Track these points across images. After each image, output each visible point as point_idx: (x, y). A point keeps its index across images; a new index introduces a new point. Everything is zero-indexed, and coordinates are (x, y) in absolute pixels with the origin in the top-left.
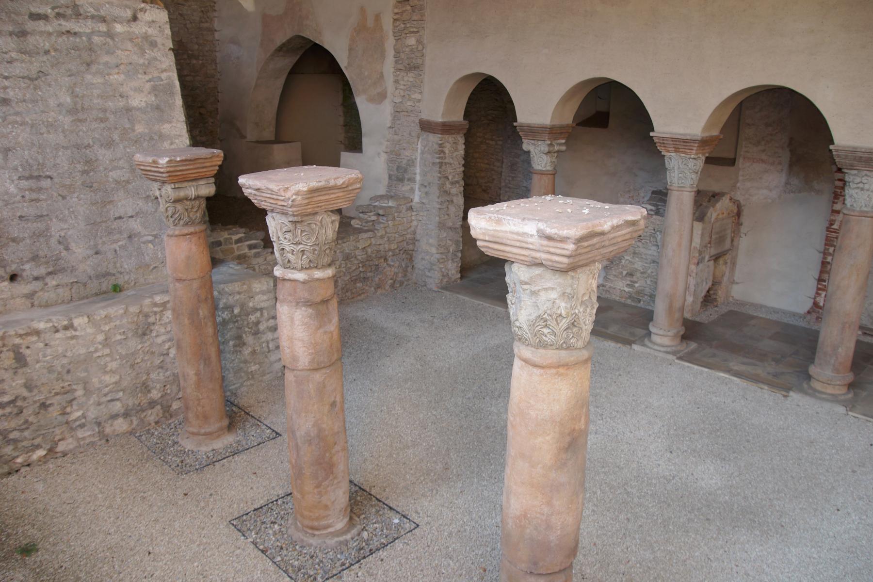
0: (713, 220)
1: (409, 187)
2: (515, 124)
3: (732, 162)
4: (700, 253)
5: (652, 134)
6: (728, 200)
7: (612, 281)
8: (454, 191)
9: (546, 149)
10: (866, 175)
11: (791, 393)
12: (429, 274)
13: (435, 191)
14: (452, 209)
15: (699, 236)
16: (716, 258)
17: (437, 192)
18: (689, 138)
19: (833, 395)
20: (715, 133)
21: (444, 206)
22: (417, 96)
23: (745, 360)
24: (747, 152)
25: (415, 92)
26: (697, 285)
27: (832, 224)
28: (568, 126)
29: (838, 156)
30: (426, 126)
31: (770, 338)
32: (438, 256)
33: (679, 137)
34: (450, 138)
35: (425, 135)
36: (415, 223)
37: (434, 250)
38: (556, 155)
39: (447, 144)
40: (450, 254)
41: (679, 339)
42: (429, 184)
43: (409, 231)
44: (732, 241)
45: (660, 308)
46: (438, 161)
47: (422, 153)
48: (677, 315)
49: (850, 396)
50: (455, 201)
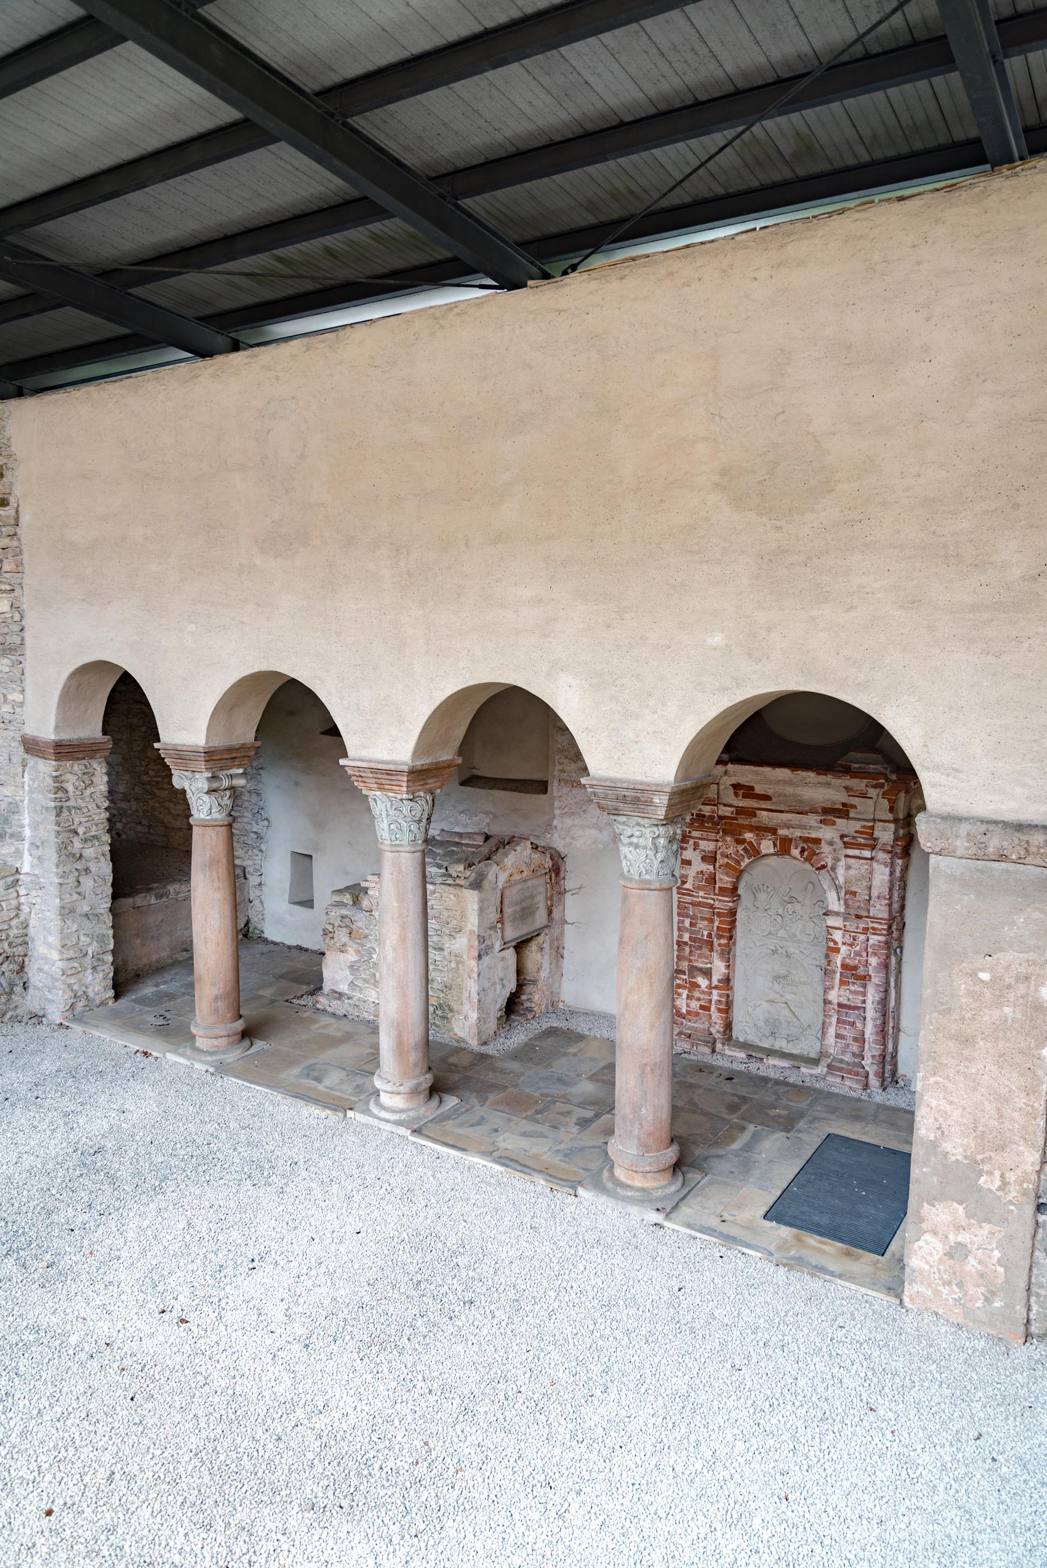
0: (500, 885)
1: (13, 849)
2: (156, 745)
3: (542, 787)
4: (481, 939)
5: (342, 762)
6: (529, 850)
7: (361, 989)
8: (89, 852)
9: (205, 786)
10: (638, 824)
11: (581, 1191)
12: (50, 997)
13: (51, 854)
14: (88, 883)
15: (476, 913)
16: (520, 946)
17: (54, 857)
18: (392, 767)
19: (643, 1190)
20: (447, 755)
21: (71, 879)
22: (17, 697)
24: (563, 771)
25: (14, 690)
26: (482, 991)
27: (684, 883)
28: (243, 747)
30: (32, 747)
31: (590, 1078)
32: (60, 964)
33: (380, 766)
34: (77, 767)
35: (32, 761)
36: (25, 909)
37: (55, 955)
38: (228, 793)
39: (69, 776)
40: (88, 959)
41: (422, 1097)
42: (43, 843)
43: (14, 923)
45: (386, 1042)
46: (53, 804)
47: (31, 792)
48: (414, 1056)
49: (673, 1188)
50: (93, 869)
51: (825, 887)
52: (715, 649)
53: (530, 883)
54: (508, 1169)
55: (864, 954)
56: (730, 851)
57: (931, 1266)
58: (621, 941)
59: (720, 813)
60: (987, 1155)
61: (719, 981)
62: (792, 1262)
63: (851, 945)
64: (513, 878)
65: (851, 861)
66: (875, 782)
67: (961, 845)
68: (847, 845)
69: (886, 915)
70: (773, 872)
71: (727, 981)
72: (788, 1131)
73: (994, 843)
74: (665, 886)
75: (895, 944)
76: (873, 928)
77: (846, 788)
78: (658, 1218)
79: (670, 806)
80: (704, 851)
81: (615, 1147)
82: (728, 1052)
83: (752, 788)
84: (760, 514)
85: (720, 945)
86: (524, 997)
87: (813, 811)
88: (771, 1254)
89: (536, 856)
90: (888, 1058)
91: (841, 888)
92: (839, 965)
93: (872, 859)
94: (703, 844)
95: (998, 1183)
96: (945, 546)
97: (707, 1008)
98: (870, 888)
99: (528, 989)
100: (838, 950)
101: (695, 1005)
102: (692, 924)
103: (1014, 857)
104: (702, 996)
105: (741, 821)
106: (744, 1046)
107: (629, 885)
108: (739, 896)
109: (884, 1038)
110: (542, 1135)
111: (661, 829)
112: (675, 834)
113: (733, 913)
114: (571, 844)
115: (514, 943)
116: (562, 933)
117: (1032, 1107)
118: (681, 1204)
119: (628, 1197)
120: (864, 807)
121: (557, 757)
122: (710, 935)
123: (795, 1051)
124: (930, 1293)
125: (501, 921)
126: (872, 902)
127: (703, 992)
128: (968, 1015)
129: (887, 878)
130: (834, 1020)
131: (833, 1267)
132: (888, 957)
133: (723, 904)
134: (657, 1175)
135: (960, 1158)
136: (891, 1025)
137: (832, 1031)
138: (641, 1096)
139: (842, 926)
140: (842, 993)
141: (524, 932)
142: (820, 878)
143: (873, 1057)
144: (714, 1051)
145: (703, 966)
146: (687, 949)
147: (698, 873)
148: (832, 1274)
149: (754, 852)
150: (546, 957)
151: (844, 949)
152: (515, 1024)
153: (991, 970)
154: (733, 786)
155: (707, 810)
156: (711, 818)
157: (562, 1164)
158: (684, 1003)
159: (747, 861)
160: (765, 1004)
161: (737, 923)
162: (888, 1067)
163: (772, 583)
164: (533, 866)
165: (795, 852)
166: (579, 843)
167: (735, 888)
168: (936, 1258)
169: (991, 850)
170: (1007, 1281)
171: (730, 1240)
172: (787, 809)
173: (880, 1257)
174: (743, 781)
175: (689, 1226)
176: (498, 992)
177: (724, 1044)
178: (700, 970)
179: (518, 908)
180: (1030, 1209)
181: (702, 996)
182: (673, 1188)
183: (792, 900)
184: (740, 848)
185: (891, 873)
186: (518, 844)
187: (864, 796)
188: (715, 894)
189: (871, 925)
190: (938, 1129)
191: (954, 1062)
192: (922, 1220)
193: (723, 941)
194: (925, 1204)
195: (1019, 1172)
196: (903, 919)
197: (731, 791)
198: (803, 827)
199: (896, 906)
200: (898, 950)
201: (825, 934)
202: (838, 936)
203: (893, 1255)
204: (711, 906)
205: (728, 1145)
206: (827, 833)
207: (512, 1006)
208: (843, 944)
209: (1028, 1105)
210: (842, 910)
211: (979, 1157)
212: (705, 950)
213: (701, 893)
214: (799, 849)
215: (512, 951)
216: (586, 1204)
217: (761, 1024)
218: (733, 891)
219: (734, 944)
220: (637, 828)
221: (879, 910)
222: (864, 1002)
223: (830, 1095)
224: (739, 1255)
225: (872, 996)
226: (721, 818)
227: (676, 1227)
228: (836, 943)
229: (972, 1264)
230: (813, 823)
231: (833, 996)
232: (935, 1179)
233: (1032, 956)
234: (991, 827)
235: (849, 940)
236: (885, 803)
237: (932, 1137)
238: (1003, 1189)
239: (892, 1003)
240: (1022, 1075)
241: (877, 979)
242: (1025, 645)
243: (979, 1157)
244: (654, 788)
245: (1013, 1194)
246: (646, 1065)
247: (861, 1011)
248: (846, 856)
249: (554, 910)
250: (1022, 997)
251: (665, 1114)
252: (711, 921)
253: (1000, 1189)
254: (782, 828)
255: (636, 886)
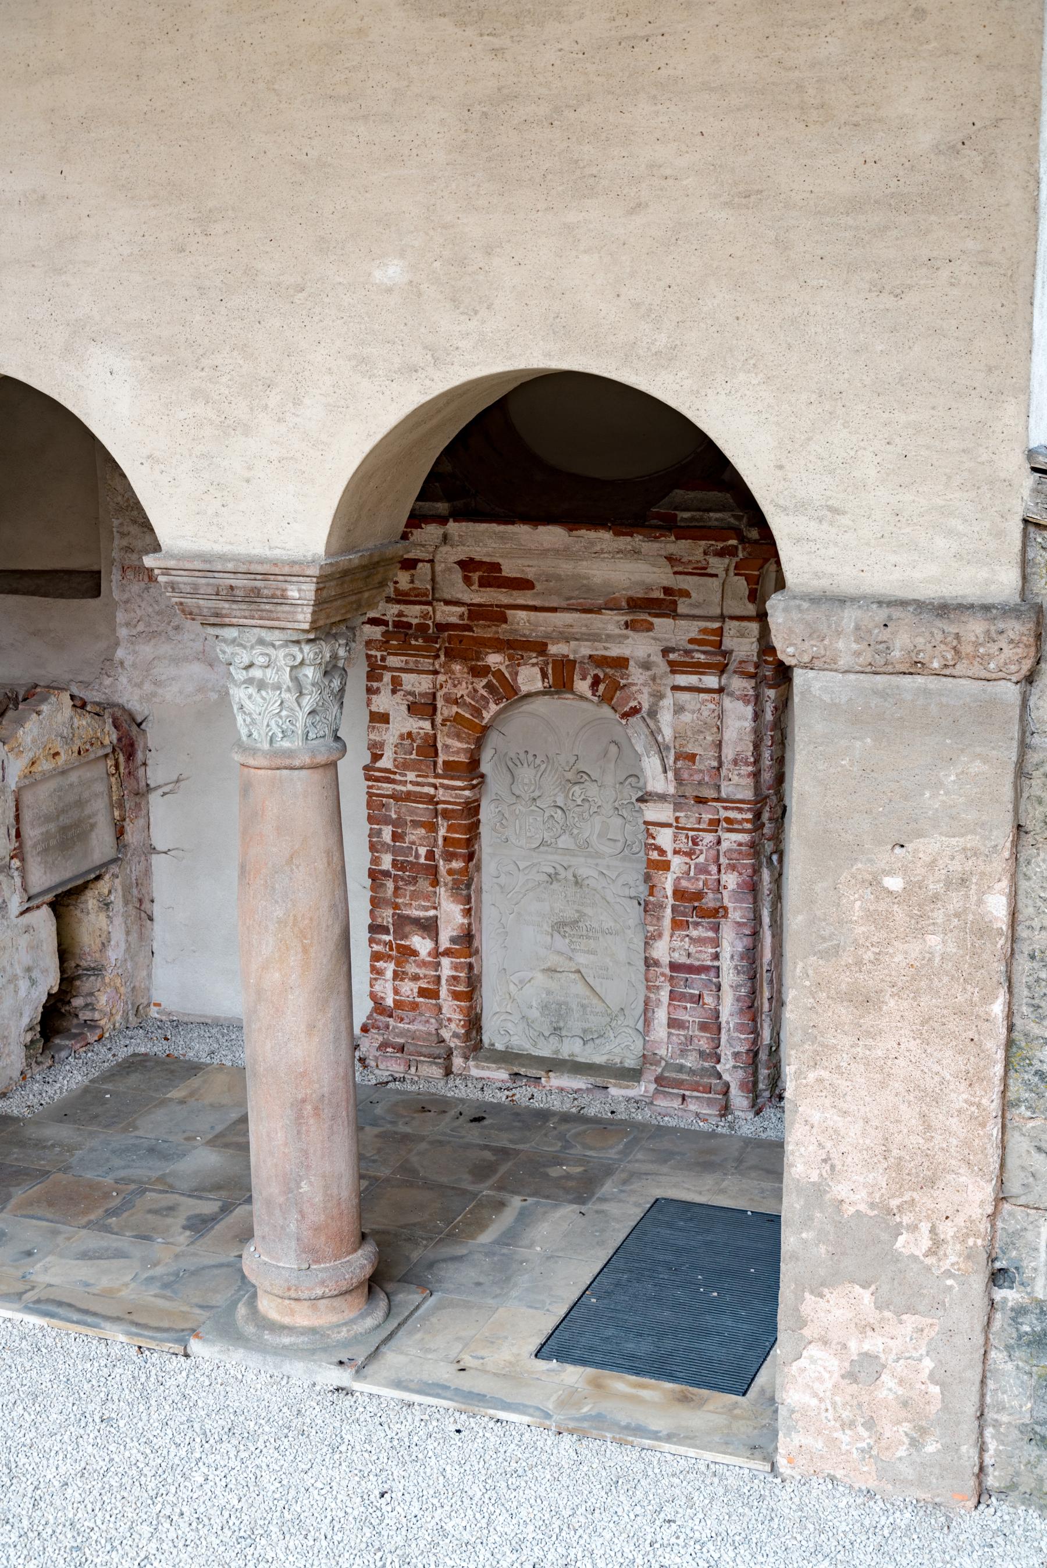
0: (12, 783)
10: (261, 642)
11: (195, 1346)
16: (63, 903)
19: (313, 1331)
23: (93, 1240)
27: (376, 757)
29: (173, 587)
31: (211, 1143)
44: (120, 832)
49: (369, 1322)
51: (639, 748)
52: (389, 290)
53: (73, 777)
54: (54, 1322)
55: (714, 869)
56: (462, 691)
57: (821, 1400)
58: (243, 870)
59: (440, 618)
60: (907, 1197)
61: (453, 940)
62: (586, 1425)
63: (689, 854)
64: (37, 768)
65: (684, 697)
66: (720, 545)
67: (845, 648)
68: (675, 667)
69: (748, 794)
70: (545, 726)
71: (467, 939)
72: (581, 1200)
73: (903, 640)
74: (321, 759)
75: (769, 847)
76: (728, 820)
77: (670, 559)
78: (343, 1377)
79: (320, 604)
80: (412, 694)
81: (255, 1260)
82: (475, 1072)
83: (496, 567)
84: (462, 24)
85: (450, 872)
86: (78, 1002)
87: (612, 606)
88: (548, 1416)
89: (83, 722)
90: (763, 1056)
91: (668, 748)
92: (669, 892)
93: (721, 690)
94: (409, 680)
95: (926, 1243)
96: (800, 88)
97: (434, 994)
98: (719, 745)
99: (86, 985)
100: (666, 866)
101: (409, 989)
102: (395, 836)
103: (936, 665)
104: (421, 972)
105: (478, 632)
106: (505, 1057)
107: (251, 762)
108: (482, 776)
109: (754, 1020)
110: (120, 1254)
111: (306, 648)
112: (335, 657)
113: (472, 809)
114: (154, 694)
115: (49, 897)
116: (148, 872)
117: (979, 1105)
118: (384, 1349)
119: (285, 1347)
120: (704, 593)
121: (116, 522)
122: (430, 855)
123: (599, 1059)
124: (820, 1445)
125: (18, 853)
126: (724, 772)
127: (424, 964)
128: (869, 955)
129: (748, 724)
130: (664, 995)
131: (656, 1424)
132: (756, 871)
133: (452, 793)
134: (337, 1302)
135: (863, 1207)
136: (767, 994)
137: (661, 1016)
138: (298, 1161)
139: (672, 821)
140: (677, 944)
141: (68, 875)
142: (630, 732)
143: (736, 1055)
144: (448, 1072)
145: (421, 914)
146: (390, 885)
147: (402, 737)
148: (655, 1436)
149: (506, 691)
150: (118, 921)
151: (677, 863)
152: (63, 1054)
153: (905, 870)
154: (461, 564)
155: (413, 613)
156: (422, 628)
157: (161, 1302)
158: (389, 986)
159: (494, 708)
160: (540, 978)
161: (483, 829)
162: (764, 1072)
163: (489, 160)
164: (78, 743)
165: (583, 686)
166: (170, 693)
167: (474, 763)
168: (829, 1385)
169: (897, 654)
170: (945, 1408)
171: (473, 1400)
172: (564, 604)
173: (739, 1398)
174: (479, 553)
175: (399, 1384)
176: (22, 993)
177: (467, 1058)
178: (417, 922)
179: (52, 827)
180: (978, 1281)
181: (421, 972)
182: (369, 1322)
183: (581, 777)
184: (480, 683)
185: (757, 716)
186: (44, 700)
187: (702, 572)
188: (437, 776)
189: (724, 814)
190: (825, 1161)
191: (847, 1041)
192: (802, 1323)
193: (457, 865)
194: (807, 1295)
195: (960, 1220)
196: (781, 799)
197: (458, 575)
198: (593, 637)
199: (767, 776)
200: (775, 858)
201: (642, 837)
202: (665, 838)
203: (763, 1391)
204: (431, 800)
205: (473, 1237)
206: (638, 647)
207: (56, 1021)
208: (676, 852)
209: (972, 1104)
210: (672, 790)
211: (894, 1203)
212: (424, 885)
213: (411, 776)
214: (589, 680)
215: (45, 912)
216: (206, 1367)
217: (535, 1013)
218: (471, 769)
219: (478, 868)
220: (259, 649)
221: (738, 785)
222: (716, 957)
223: (661, 1131)
224: (491, 1424)
225: (731, 944)
226: (441, 627)
227: (375, 1390)
228: (662, 852)
229: (888, 1387)
230: (613, 629)
231: (661, 951)
232: (823, 1249)
233: (971, 841)
234: (897, 612)
235: (685, 845)
236: (741, 585)
237: (814, 1177)
238: (935, 1253)
239: (767, 955)
240: (961, 1052)
241: (737, 912)
242: (944, 274)
243: (894, 1203)
244: (286, 570)
245: (952, 1257)
246: (304, 1101)
247: (712, 974)
248: (676, 688)
249: (129, 827)
250: (957, 915)
251: (345, 1189)
252: (432, 827)
253: (930, 1252)
254: (556, 641)
255: (263, 762)
